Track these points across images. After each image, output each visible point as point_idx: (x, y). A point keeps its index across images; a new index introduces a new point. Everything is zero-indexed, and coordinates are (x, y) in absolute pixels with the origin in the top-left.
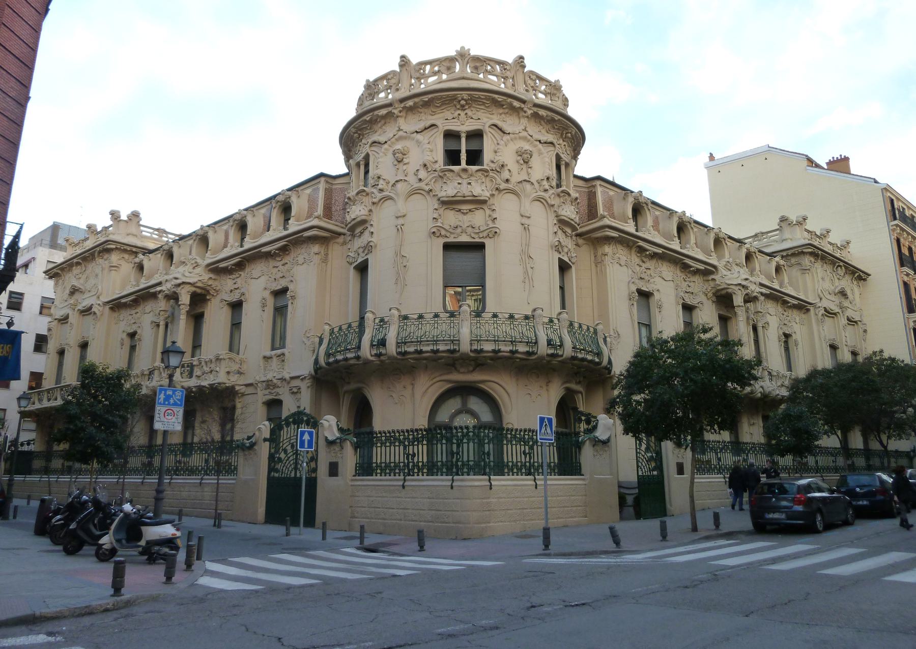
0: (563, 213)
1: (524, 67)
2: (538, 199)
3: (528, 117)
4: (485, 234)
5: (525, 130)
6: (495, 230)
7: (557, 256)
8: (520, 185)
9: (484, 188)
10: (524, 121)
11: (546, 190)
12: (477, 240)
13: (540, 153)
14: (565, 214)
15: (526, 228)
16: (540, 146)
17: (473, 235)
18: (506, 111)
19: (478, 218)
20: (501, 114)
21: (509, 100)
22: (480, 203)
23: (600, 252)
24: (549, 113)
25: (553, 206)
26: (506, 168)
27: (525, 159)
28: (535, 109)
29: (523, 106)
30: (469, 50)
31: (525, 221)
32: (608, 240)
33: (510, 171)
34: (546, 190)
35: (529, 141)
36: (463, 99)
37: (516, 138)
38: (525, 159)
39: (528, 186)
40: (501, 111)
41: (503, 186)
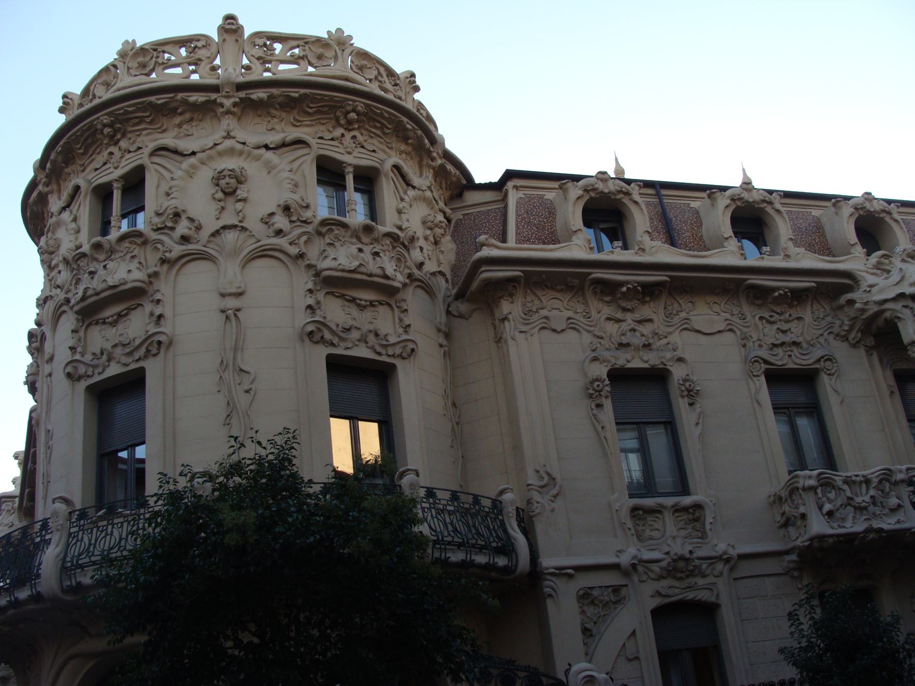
0: (328, 263)
1: (239, 30)
2: (263, 253)
3: (228, 112)
4: (142, 351)
5: (228, 136)
6: (156, 338)
7: (322, 352)
8: (216, 239)
9: (134, 265)
10: (228, 123)
11: (279, 232)
12: (133, 366)
13: (270, 168)
14: (333, 264)
15: (231, 316)
16: (269, 155)
17: (124, 360)
18: (187, 116)
19: (136, 326)
20: (179, 126)
21: (180, 96)
22: (131, 296)
23: (498, 315)
24: (275, 91)
25: (301, 256)
26: (184, 217)
27: (229, 188)
28: (242, 94)
29: (213, 96)
30: (134, 41)
31: (231, 303)
32: (505, 287)
33: (191, 220)
34: (279, 232)
35: (241, 153)
36: (105, 126)
37: (210, 158)
38: (229, 188)
39: (230, 237)
40: (177, 120)
41: (178, 250)
